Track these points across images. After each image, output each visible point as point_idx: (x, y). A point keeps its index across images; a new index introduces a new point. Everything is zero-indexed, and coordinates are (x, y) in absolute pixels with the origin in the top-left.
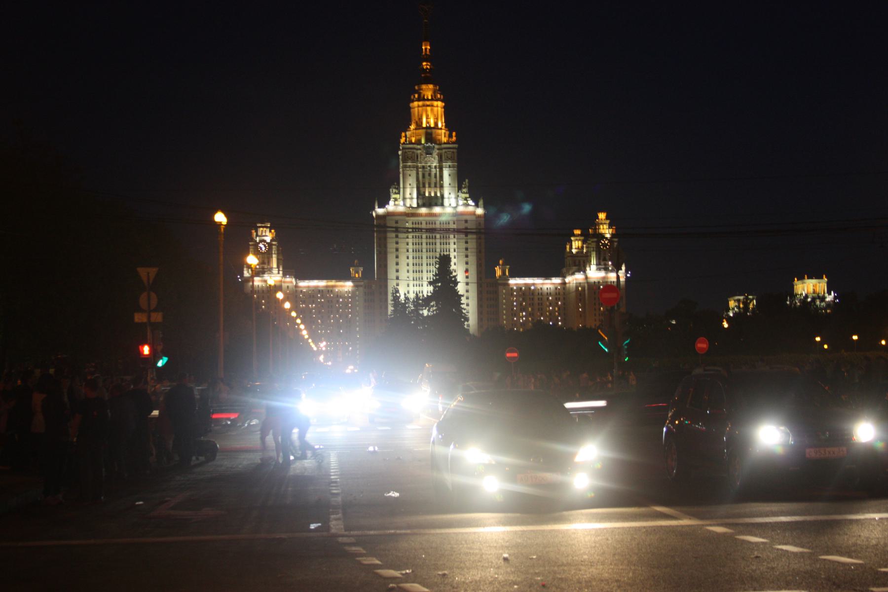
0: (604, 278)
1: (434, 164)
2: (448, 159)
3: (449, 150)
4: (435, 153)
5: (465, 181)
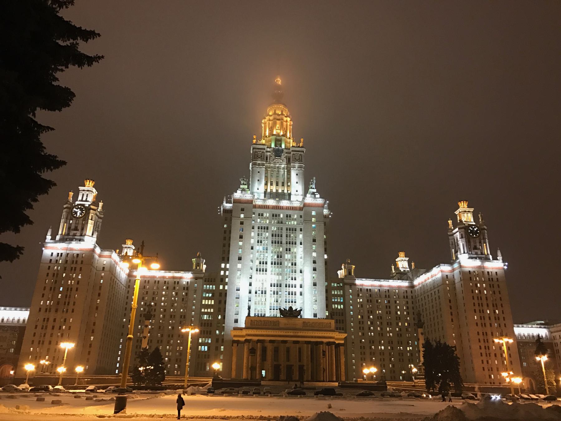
0: (479, 267)
1: (283, 166)
2: (295, 160)
3: (297, 153)
4: (283, 156)
5: (313, 179)
